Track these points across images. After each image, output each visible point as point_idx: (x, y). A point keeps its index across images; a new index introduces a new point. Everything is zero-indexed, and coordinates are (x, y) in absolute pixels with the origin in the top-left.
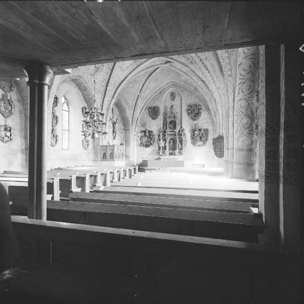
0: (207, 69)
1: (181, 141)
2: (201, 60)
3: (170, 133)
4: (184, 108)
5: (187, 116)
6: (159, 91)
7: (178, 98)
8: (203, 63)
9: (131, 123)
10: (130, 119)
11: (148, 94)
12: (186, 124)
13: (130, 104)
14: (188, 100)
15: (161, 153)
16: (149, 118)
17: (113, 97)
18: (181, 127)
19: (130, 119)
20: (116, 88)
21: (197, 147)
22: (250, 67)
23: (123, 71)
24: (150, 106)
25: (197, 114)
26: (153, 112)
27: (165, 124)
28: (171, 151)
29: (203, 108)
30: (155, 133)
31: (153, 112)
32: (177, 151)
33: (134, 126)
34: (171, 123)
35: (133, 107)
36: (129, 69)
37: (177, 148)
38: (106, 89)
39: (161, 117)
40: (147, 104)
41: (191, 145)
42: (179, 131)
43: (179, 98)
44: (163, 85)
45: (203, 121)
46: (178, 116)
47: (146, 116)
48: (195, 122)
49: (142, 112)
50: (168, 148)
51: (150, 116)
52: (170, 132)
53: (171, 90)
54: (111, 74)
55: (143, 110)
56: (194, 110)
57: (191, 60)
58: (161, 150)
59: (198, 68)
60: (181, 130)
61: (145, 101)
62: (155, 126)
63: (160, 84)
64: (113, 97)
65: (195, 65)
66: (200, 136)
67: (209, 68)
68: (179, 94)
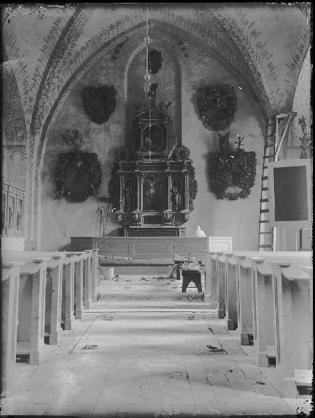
1: (179, 184)
4: (187, 97)
6: (113, 45)
11: (83, 49)
12: (195, 138)
14: (198, 72)
15: (120, 218)
18: (180, 145)
19: (28, 117)
21: (224, 203)
24: (86, 83)
25: (224, 111)
26: (97, 102)
27: (133, 135)
28: (152, 214)
30: (104, 157)
31: (97, 102)
32: (169, 212)
33: (38, 138)
34: (152, 130)
35: (39, 81)
37: (170, 204)
39: (118, 115)
40: (79, 78)
41: (210, 196)
42: (174, 157)
45: (247, 134)
46: (172, 112)
48: (223, 133)
50: (141, 202)
51: (87, 113)
55: (67, 94)
56: (215, 101)
58: (122, 211)
60: (184, 153)
61: (75, 67)
62: (103, 141)
66: (230, 172)
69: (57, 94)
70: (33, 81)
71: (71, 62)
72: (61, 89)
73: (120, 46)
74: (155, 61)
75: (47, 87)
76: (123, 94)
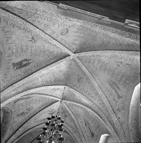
0: (84, 138)
2: (82, 131)
8: (83, 134)
17: (18, 137)
20: (24, 131)
22: (136, 133)
23: (35, 122)
36: (39, 122)
38: (18, 129)
54: (28, 120)
57: (75, 130)
59: (78, 136)
64: (18, 137)
65: (77, 134)
67: (86, 138)
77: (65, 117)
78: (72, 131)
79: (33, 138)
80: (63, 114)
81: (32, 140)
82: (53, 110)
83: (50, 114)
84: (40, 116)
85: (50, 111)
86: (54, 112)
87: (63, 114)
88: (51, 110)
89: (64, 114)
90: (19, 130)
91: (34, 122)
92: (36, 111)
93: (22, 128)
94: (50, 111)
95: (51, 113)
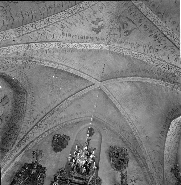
3: (77, 180)
5: (107, 161)
6: (76, 121)
7: (96, 135)
9: (17, 141)
10: (21, 135)
13: (35, 114)
16: (50, 147)
23: (63, 34)
25: (122, 160)
29: (130, 154)
43: (98, 136)
44: (83, 115)
47: (46, 143)
49: (43, 136)
52: (76, 178)
53: (90, 125)
55: (46, 134)
61: (55, 124)
63: (80, 113)
68: (99, 132)
69: (42, 133)
70: (33, 120)
71: (55, 121)
72: (45, 131)
73: (78, 123)
74: (91, 132)
75: (39, 125)
76: (71, 143)
77: (125, 35)
78: (149, 51)
79: (61, 97)
80: (122, 30)
81: (61, 101)
82: (99, 20)
83: (93, 29)
84: (73, 25)
85: (93, 22)
86: (102, 27)
87: (122, 30)
88: (95, 20)
89: (122, 31)
90: (27, 28)
91: (61, 32)
92: (64, 6)
93: (34, 26)
94: (93, 22)
95: (96, 29)
